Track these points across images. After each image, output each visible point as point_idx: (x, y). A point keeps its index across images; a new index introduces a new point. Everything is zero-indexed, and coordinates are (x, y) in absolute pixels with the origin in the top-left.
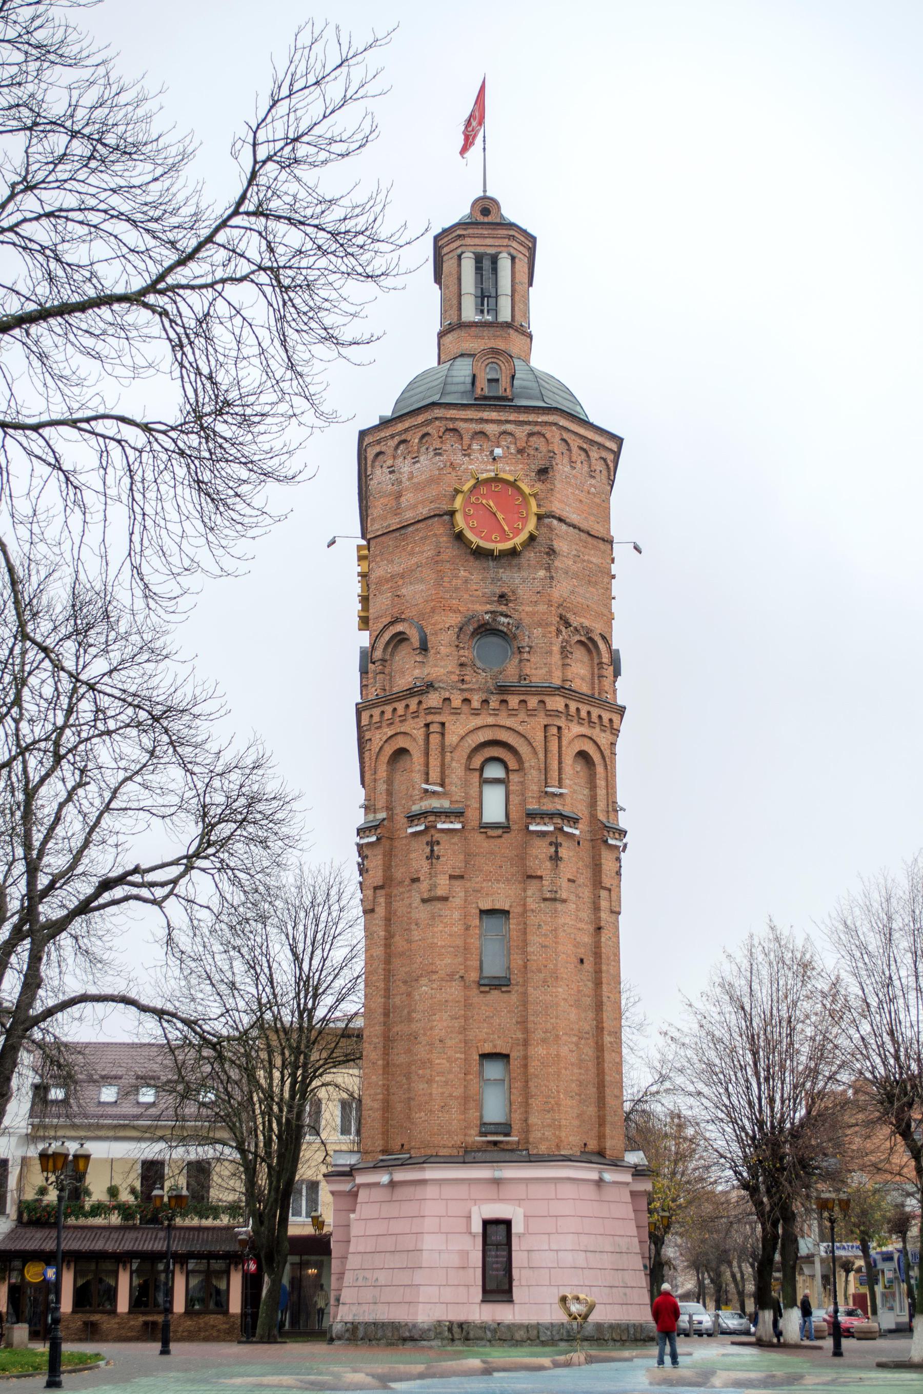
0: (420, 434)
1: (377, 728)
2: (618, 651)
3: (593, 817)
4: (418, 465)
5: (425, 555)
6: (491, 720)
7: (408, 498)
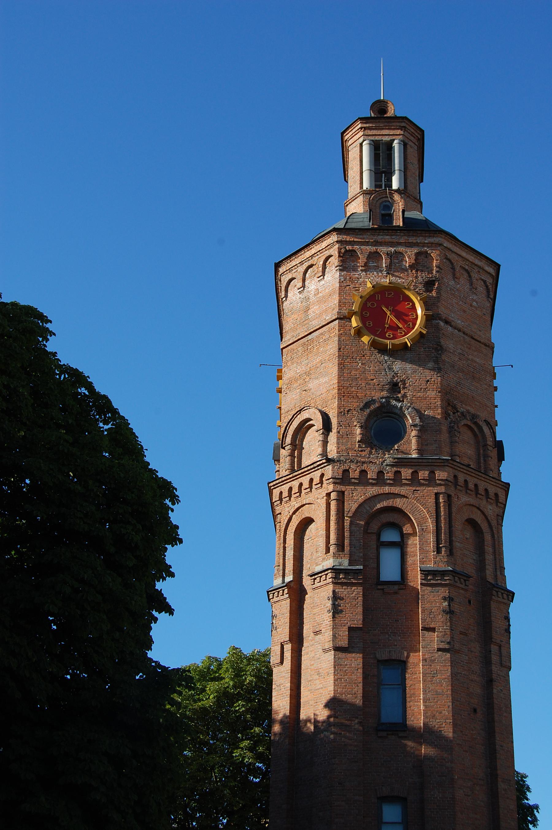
0: (324, 258)
1: (286, 502)
2: (501, 441)
3: (483, 579)
4: (323, 282)
5: (328, 353)
6: (387, 489)
7: (315, 310)
